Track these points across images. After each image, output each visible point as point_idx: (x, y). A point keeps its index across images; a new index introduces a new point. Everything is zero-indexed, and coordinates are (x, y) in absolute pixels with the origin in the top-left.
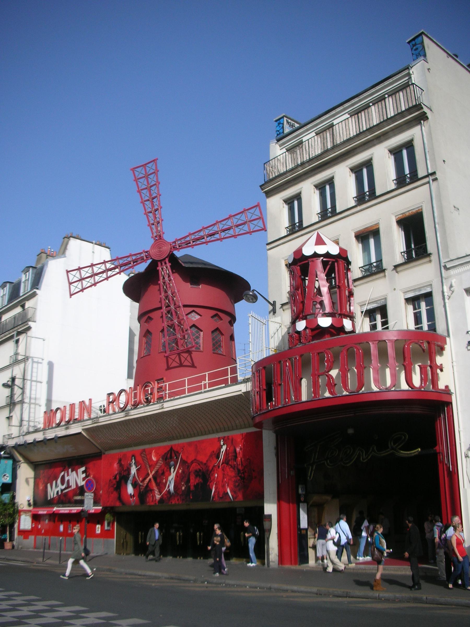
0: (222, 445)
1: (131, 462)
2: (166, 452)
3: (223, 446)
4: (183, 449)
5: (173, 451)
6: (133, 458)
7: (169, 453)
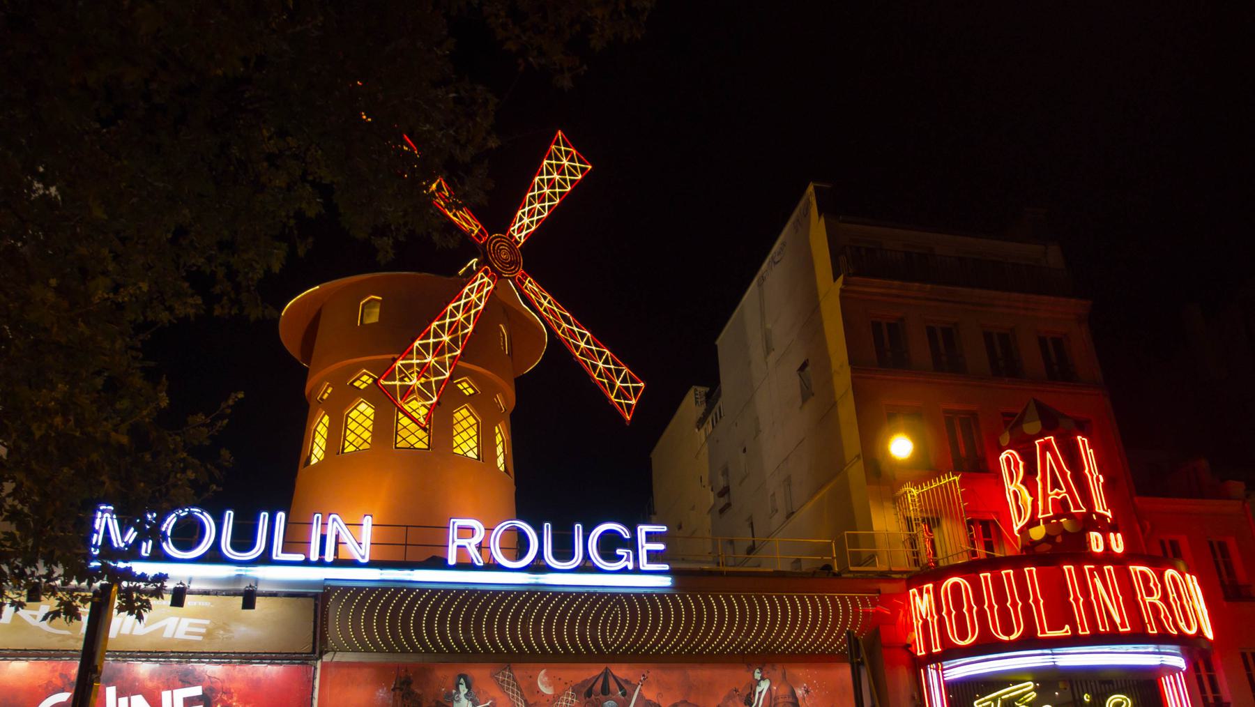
0: (759, 679)
1: (454, 691)
2: (588, 678)
3: (762, 682)
4: (644, 675)
5: (611, 681)
6: (462, 680)
7: (600, 681)
